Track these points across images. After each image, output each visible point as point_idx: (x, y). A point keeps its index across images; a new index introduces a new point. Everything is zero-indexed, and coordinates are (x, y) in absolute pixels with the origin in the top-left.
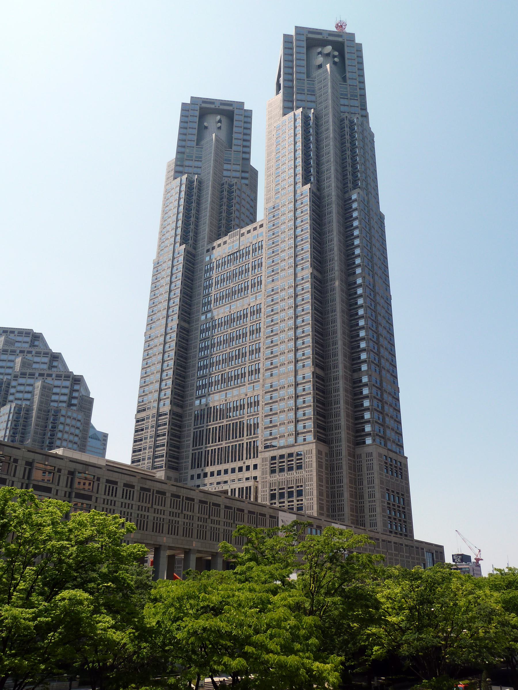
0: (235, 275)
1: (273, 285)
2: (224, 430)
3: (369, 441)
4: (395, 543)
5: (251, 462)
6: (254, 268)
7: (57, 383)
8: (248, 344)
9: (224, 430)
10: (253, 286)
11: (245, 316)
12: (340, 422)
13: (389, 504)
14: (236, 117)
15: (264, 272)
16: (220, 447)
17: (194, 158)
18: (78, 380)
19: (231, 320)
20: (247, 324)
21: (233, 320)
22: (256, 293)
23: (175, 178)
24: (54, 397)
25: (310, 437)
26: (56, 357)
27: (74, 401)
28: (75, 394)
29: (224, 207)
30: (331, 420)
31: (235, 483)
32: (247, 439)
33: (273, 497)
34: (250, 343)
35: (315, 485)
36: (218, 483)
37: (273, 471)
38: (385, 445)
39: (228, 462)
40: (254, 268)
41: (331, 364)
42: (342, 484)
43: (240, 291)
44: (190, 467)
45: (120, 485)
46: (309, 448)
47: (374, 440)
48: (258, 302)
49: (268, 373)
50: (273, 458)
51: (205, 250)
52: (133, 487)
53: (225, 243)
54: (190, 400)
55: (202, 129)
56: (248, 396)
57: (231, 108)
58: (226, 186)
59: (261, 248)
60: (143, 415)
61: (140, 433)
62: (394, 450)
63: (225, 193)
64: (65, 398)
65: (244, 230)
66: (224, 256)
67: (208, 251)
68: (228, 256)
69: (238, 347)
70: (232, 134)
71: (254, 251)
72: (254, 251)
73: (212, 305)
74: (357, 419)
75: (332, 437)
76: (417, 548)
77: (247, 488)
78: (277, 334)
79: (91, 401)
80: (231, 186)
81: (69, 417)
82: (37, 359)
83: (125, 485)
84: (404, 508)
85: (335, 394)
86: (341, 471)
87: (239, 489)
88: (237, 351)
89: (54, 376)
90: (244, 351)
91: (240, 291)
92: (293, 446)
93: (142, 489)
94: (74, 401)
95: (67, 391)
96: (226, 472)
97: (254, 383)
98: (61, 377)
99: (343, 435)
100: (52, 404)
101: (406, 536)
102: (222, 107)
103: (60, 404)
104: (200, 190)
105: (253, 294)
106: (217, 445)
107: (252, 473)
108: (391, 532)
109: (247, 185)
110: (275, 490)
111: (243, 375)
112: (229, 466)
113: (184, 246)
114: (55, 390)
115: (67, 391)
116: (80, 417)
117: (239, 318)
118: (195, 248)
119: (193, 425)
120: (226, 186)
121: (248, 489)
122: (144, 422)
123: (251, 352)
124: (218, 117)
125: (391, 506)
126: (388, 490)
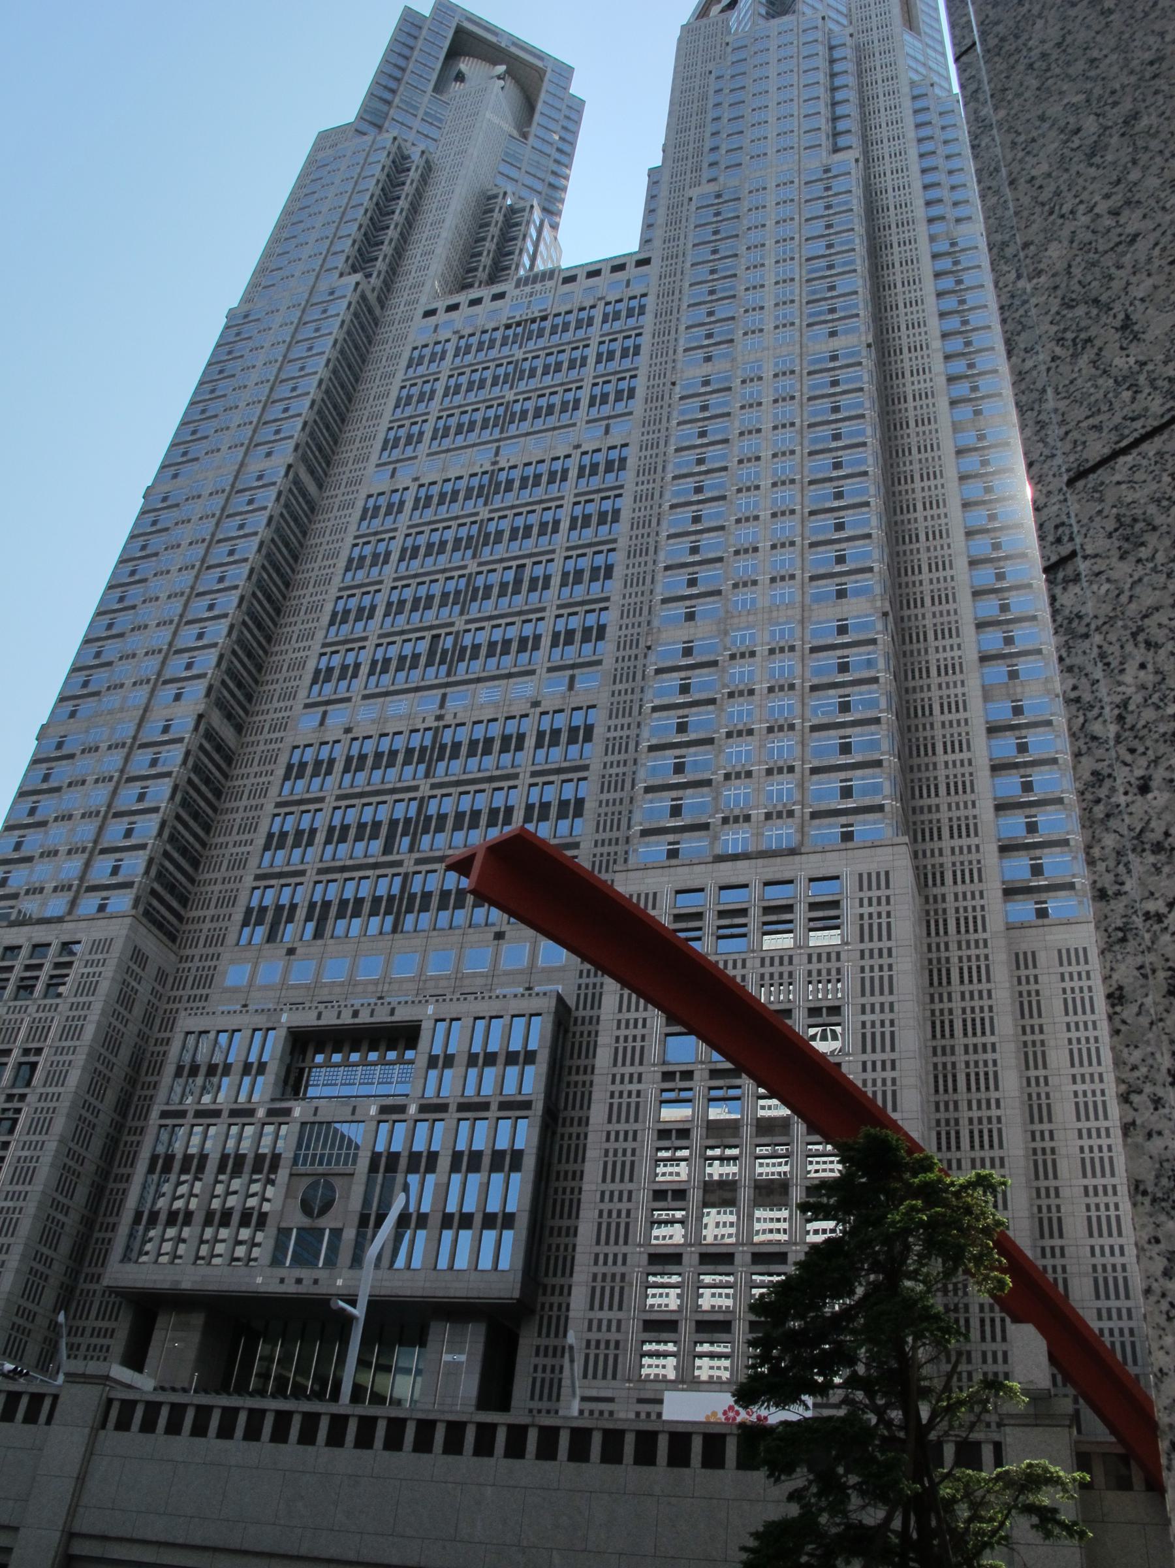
1: (707, 369)
12: (976, 812)
14: (546, 85)
17: (420, 114)
30: (926, 802)
41: (929, 622)
42: (989, 1039)
48: (615, 439)
51: (420, 312)
55: (449, 75)
57: (540, 64)
67: (430, 313)
68: (508, 327)
75: (937, 860)
85: (947, 717)
86: (984, 986)
92: (793, 852)
102: (513, 49)
104: (424, 179)
118: (382, 303)
124: (501, 69)
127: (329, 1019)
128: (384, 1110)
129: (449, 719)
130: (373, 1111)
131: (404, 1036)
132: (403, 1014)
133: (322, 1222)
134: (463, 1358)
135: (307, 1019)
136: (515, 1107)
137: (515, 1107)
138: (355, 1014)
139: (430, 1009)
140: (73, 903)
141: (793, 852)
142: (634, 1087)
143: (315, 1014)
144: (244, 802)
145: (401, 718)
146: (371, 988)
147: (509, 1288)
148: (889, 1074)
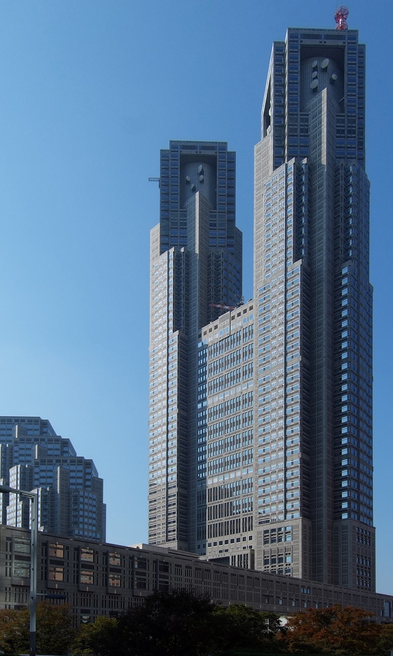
0: (227, 363)
2: (224, 509)
3: (345, 516)
4: (362, 596)
5: (247, 534)
6: (245, 354)
7: (73, 468)
8: (240, 431)
9: (224, 509)
10: (245, 373)
11: (238, 404)
13: (358, 566)
15: (255, 359)
16: (221, 522)
18: (89, 464)
19: (225, 408)
20: (240, 412)
21: (227, 408)
22: (248, 381)
23: (162, 252)
24: (72, 481)
25: (297, 515)
26: (66, 443)
27: (88, 483)
28: (88, 477)
29: (212, 284)
31: (235, 550)
32: (243, 515)
33: (266, 562)
34: (243, 430)
35: (300, 553)
36: (221, 552)
37: (266, 542)
38: (359, 519)
39: (228, 534)
40: (245, 354)
43: (232, 379)
44: (196, 539)
45: (184, 567)
46: (295, 521)
47: (349, 516)
49: (261, 459)
50: (266, 532)
52: (191, 568)
53: (216, 327)
54: (193, 482)
56: (243, 478)
58: (213, 258)
59: (251, 333)
60: (154, 497)
61: (153, 512)
62: (365, 522)
63: (213, 267)
64: (80, 481)
65: (234, 313)
66: (215, 342)
69: (232, 434)
70: (216, 188)
71: (245, 335)
72: (245, 335)
73: (207, 393)
74: (335, 497)
76: (378, 599)
77: (244, 555)
78: (268, 423)
79: (101, 481)
80: (218, 257)
81: (86, 497)
82: (50, 446)
83: (186, 567)
84: (369, 569)
87: (238, 556)
88: (232, 438)
89: (69, 462)
90: (238, 438)
91: (232, 379)
93: (196, 569)
94: (88, 483)
95: (81, 474)
96: (226, 542)
97: (247, 467)
98: (75, 462)
99: (325, 511)
100: (71, 487)
101: (370, 590)
103: (78, 487)
105: (245, 382)
106: (218, 521)
107: (249, 543)
108: (358, 587)
109: (233, 254)
110: (268, 557)
111: (238, 460)
112: (229, 537)
113: (177, 332)
114: (72, 474)
115: (81, 474)
116: (95, 497)
117: (232, 406)
119: (197, 504)
120: (213, 258)
121: (246, 555)
122: (157, 502)
123: (245, 439)
125: (360, 567)
126: (358, 555)
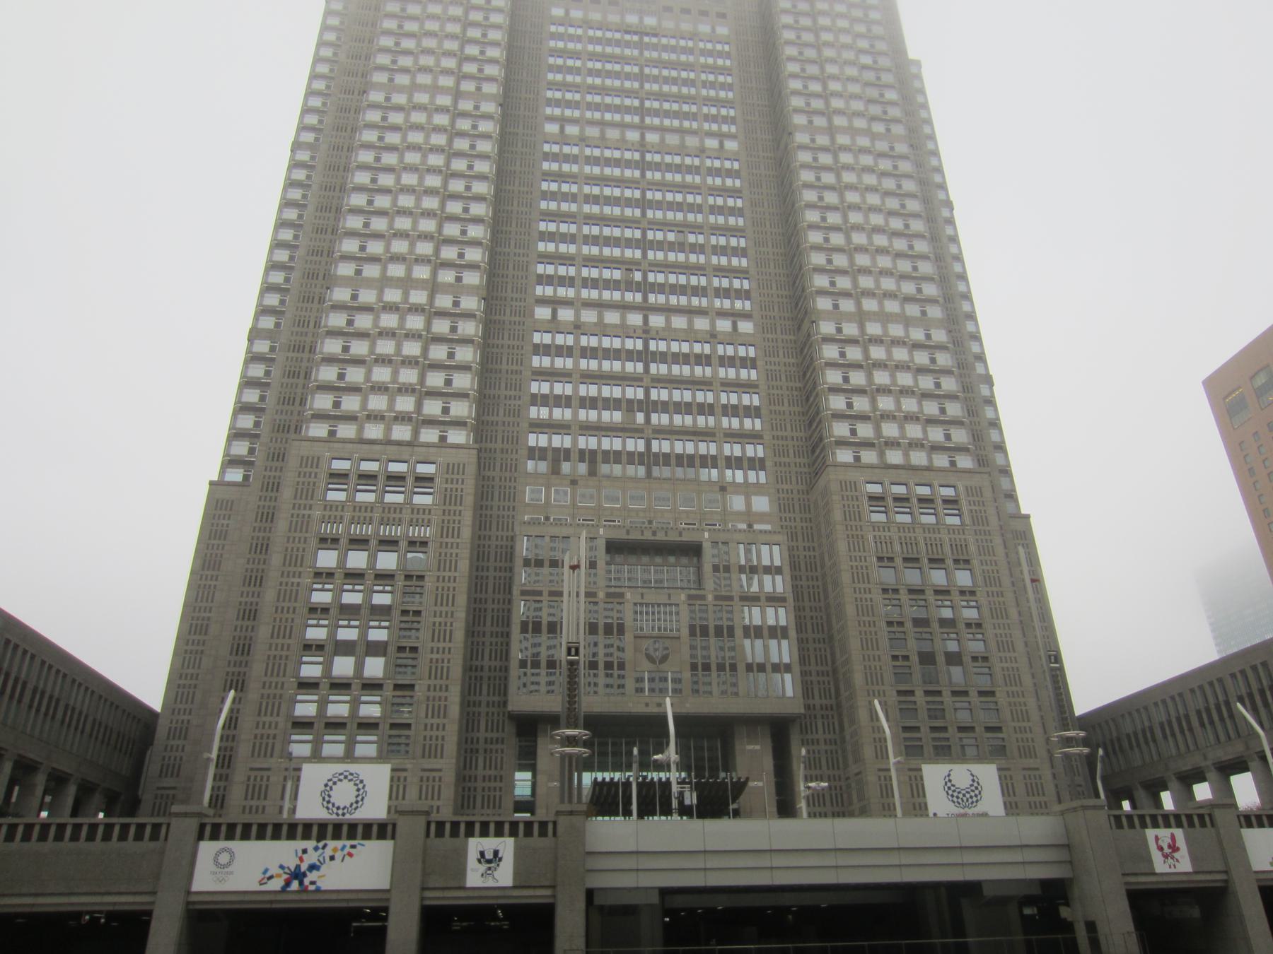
127: (635, 536)
128: (690, 597)
129: (653, 334)
130: (683, 597)
131: (693, 550)
132: (686, 537)
133: (664, 667)
134: (758, 747)
135: (621, 535)
136: (774, 600)
137: (774, 600)
138: (654, 533)
139: (706, 535)
140: (416, 433)
141: (929, 468)
142: (868, 596)
143: (624, 531)
144: (504, 367)
145: (616, 326)
146: (641, 514)
147: (798, 708)
148: (1001, 599)
